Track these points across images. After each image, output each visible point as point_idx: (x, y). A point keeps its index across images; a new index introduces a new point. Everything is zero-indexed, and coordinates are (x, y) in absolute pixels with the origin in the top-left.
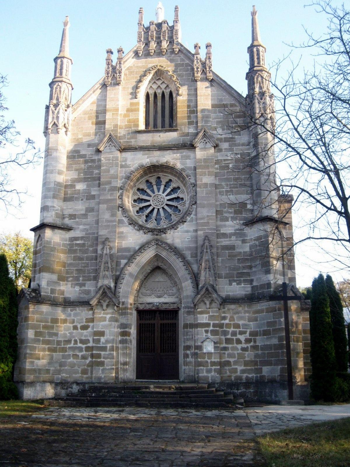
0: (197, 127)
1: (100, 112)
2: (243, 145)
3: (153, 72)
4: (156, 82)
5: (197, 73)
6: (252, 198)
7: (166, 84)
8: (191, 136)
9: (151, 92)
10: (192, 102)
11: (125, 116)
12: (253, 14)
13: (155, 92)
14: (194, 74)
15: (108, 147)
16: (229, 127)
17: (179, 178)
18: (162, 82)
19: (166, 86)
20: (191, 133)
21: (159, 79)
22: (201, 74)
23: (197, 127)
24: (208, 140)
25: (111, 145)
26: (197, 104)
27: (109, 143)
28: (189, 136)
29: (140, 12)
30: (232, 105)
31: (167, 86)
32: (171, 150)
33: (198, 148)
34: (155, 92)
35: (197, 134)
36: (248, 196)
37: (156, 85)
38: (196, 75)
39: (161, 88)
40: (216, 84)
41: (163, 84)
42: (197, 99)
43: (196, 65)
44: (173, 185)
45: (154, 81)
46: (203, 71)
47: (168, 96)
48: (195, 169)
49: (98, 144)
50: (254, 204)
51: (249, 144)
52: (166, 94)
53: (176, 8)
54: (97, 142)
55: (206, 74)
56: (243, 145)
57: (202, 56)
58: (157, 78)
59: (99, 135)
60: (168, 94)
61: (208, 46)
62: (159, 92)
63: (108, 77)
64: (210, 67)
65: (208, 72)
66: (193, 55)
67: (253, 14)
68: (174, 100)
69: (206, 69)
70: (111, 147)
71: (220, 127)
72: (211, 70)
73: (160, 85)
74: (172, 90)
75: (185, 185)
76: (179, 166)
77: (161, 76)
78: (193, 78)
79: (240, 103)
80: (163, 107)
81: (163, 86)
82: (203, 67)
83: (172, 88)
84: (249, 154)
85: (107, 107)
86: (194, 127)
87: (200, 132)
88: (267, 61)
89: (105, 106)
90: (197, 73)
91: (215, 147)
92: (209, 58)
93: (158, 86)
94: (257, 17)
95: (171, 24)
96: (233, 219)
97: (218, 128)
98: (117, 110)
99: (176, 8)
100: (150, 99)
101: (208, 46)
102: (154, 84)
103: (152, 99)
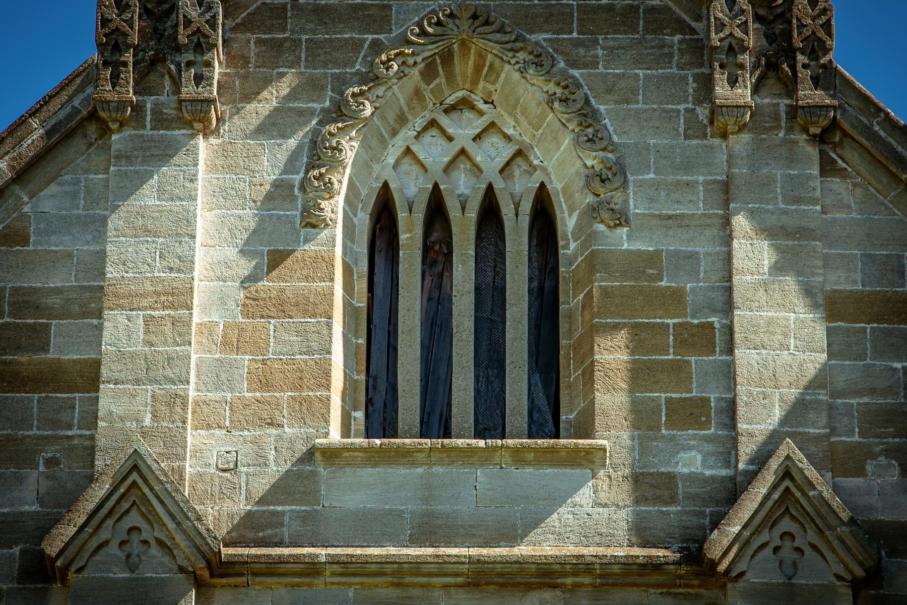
1: (54, 301)
4: (444, 120)
5: (733, 82)
7: (508, 138)
8: (688, 497)
9: (411, 188)
10: (694, 273)
11: (234, 341)
13: (436, 186)
14: (706, 84)
15: (113, 549)
18: (480, 123)
19: (508, 152)
20: (691, 478)
21: (465, 104)
22: (756, 90)
23: (734, 442)
24: (812, 536)
25: (135, 537)
26: (730, 290)
27: (127, 523)
28: (673, 500)
31: (519, 153)
32: (555, 586)
33: (741, 584)
34: (436, 186)
35: (732, 492)
37: (441, 141)
38: (722, 90)
39: (477, 169)
40: (848, 153)
41: (494, 139)
42: (728, 258)
43: (721, 26)
45: (428, 116)
46: (772, 66)
47: (525, 221)
49: (45, 525)
52: (507, 210)
54: (35, 508)
55: (790, 87)
58: (451, 100)
59: (50, 462)
60: (526, 207)
62: (463, 187)
63: (117, 67)
64: (816, 48)
65: (804, 75)
68: (569, 248)
69: (790, 54)
70: (135, 546)
71: (888, 452)
72: (828, 68)
73: (471, 148)
74: (556, 186)
77: (475, 82)
78: (702, 113)
80: (490, 297)
81: (491, 155)
82: (770, 38)
85: (112, 272)
86: (709, 439)
87: (751, 477)
89: (101, 257)
90: (733, 82)
91: (856, 585)
93: (455, 148)
97: (874, 457)
98: (180, 298)
100: (403, 237)
102: (432, 139)
103: (410, 234)
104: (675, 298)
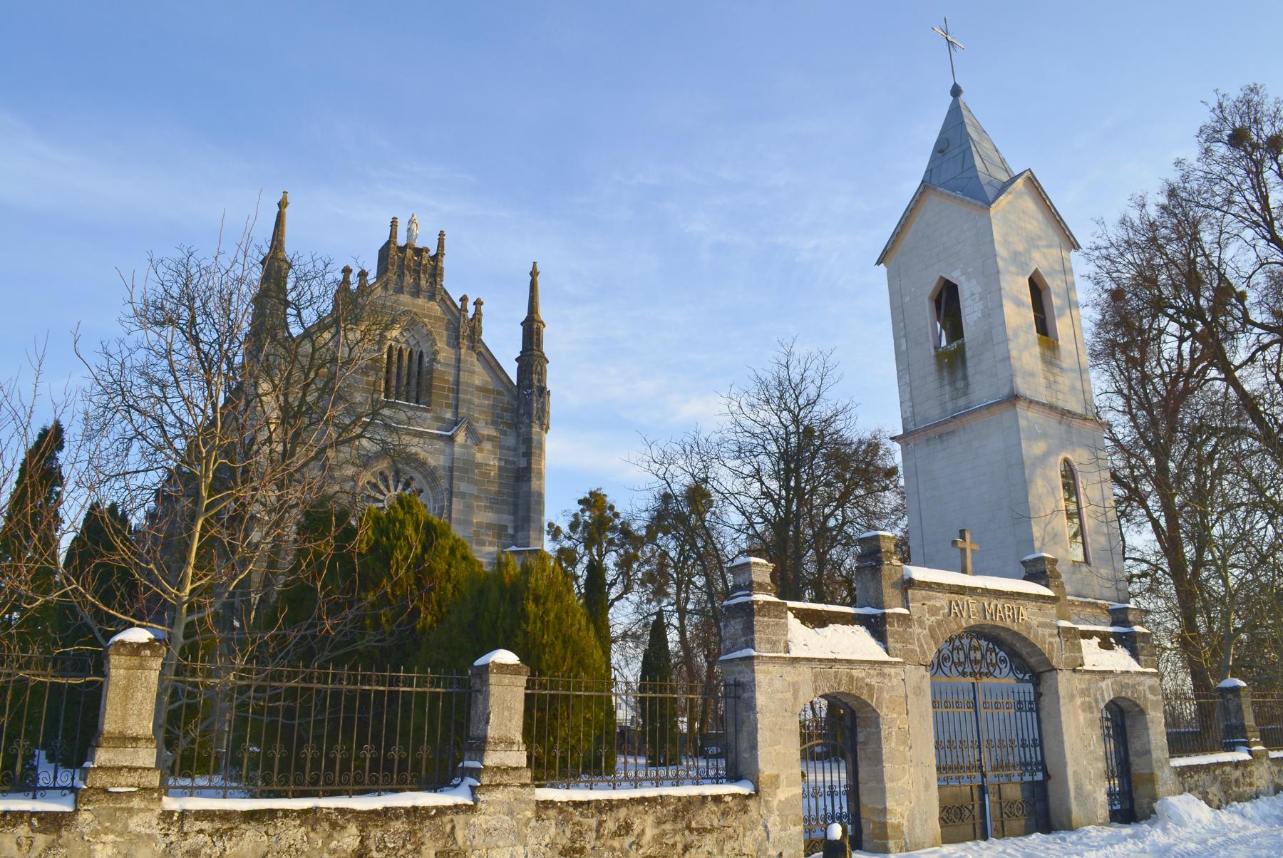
0: (456, 413)
2: (508, 449)
3: (405, 320)
6: (515, 521)
12: (534, 274)
16: (494, 423)
17: (425, 477)
29: (394, 223)
30: (499, 393)
36: (511, 517)
44: (414, 485)
48: (451, 470)
50: (516, 529)
51: (515, 449)
53: (442, 234)
56: (508, 449)
57: (470, 315)
61: (478, 303)
66: (460, 311)
67: (534, 274)
75: (431, 488)
76: (432, 462)
79: (509, 391)
81: (412, 342)
83: (425, 347)
84: (514, 463)
88: (551, 345)
92: (480, 321)
94: (539, 279)
95: (433, 252)
96: (491, 544)
99: (442, 234)
101: (478, 303)
103: (395, 357)
104: (447, 382)
